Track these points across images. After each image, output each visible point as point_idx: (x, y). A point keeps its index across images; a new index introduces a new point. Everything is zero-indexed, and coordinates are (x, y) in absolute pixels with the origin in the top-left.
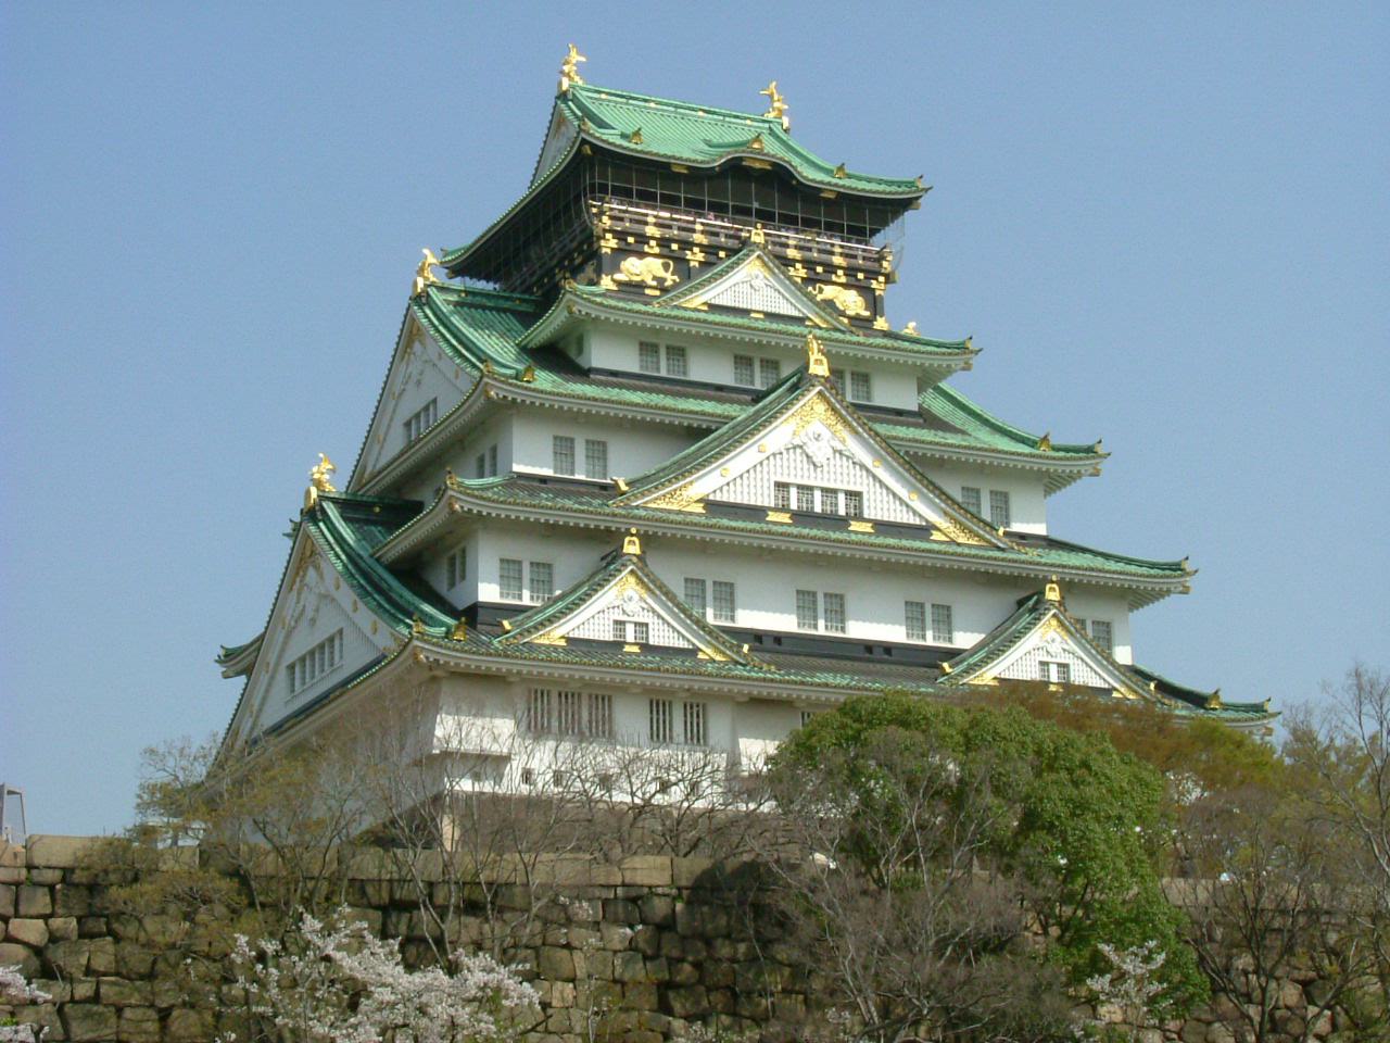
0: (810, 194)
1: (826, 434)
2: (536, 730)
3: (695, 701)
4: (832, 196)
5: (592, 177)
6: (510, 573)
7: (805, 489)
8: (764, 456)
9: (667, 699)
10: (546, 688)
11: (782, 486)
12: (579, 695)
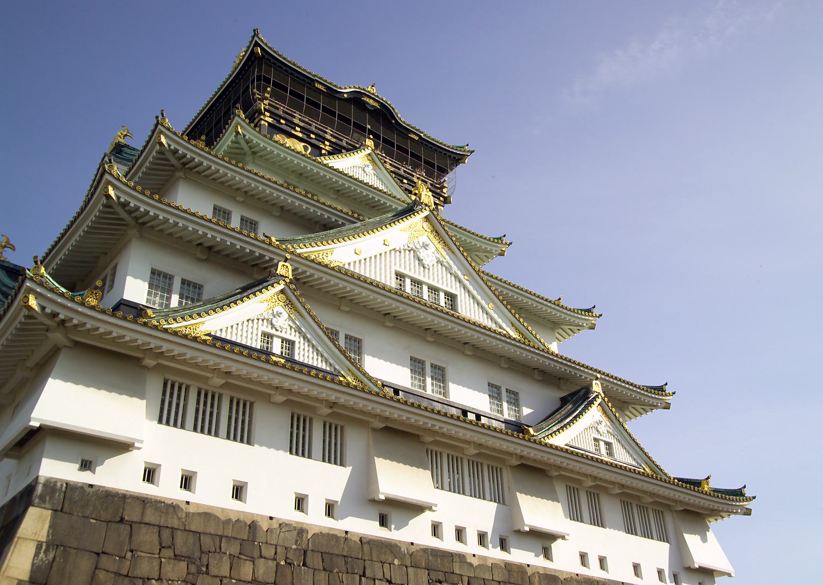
0: (403, 131)
1: (432, 248)
2: (169, 415)
3: (334, 421)
4: (417, 138)
5: (260, 70)
6: (160, 281)
7: (416, 282)
8: (387, 249)
9: (308, 414)
10: (186, 381)
11: (400, 276)
12: (220, 396)
